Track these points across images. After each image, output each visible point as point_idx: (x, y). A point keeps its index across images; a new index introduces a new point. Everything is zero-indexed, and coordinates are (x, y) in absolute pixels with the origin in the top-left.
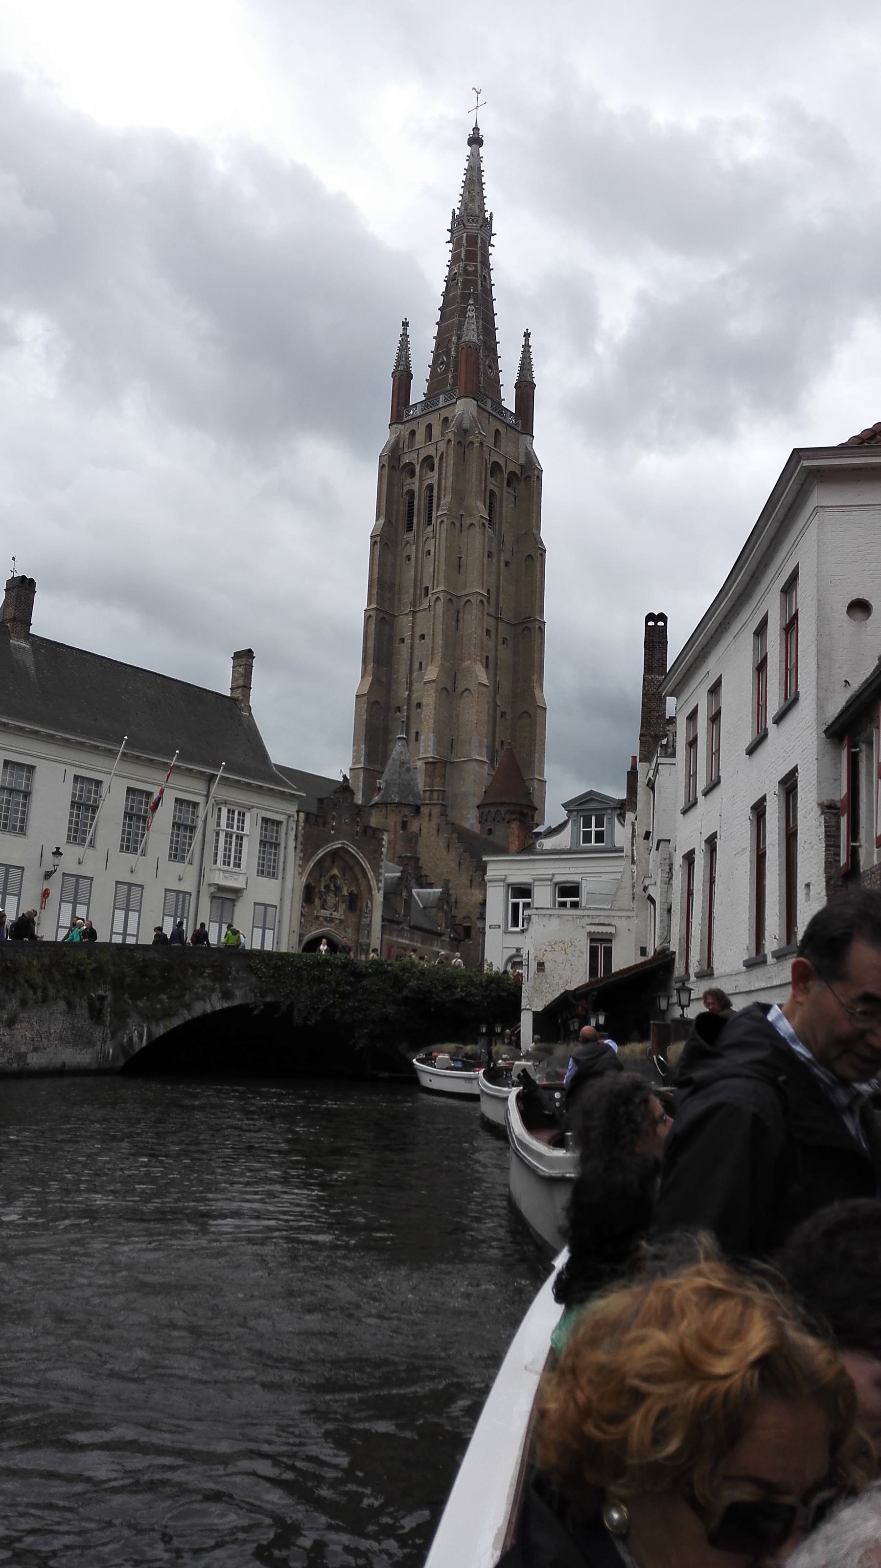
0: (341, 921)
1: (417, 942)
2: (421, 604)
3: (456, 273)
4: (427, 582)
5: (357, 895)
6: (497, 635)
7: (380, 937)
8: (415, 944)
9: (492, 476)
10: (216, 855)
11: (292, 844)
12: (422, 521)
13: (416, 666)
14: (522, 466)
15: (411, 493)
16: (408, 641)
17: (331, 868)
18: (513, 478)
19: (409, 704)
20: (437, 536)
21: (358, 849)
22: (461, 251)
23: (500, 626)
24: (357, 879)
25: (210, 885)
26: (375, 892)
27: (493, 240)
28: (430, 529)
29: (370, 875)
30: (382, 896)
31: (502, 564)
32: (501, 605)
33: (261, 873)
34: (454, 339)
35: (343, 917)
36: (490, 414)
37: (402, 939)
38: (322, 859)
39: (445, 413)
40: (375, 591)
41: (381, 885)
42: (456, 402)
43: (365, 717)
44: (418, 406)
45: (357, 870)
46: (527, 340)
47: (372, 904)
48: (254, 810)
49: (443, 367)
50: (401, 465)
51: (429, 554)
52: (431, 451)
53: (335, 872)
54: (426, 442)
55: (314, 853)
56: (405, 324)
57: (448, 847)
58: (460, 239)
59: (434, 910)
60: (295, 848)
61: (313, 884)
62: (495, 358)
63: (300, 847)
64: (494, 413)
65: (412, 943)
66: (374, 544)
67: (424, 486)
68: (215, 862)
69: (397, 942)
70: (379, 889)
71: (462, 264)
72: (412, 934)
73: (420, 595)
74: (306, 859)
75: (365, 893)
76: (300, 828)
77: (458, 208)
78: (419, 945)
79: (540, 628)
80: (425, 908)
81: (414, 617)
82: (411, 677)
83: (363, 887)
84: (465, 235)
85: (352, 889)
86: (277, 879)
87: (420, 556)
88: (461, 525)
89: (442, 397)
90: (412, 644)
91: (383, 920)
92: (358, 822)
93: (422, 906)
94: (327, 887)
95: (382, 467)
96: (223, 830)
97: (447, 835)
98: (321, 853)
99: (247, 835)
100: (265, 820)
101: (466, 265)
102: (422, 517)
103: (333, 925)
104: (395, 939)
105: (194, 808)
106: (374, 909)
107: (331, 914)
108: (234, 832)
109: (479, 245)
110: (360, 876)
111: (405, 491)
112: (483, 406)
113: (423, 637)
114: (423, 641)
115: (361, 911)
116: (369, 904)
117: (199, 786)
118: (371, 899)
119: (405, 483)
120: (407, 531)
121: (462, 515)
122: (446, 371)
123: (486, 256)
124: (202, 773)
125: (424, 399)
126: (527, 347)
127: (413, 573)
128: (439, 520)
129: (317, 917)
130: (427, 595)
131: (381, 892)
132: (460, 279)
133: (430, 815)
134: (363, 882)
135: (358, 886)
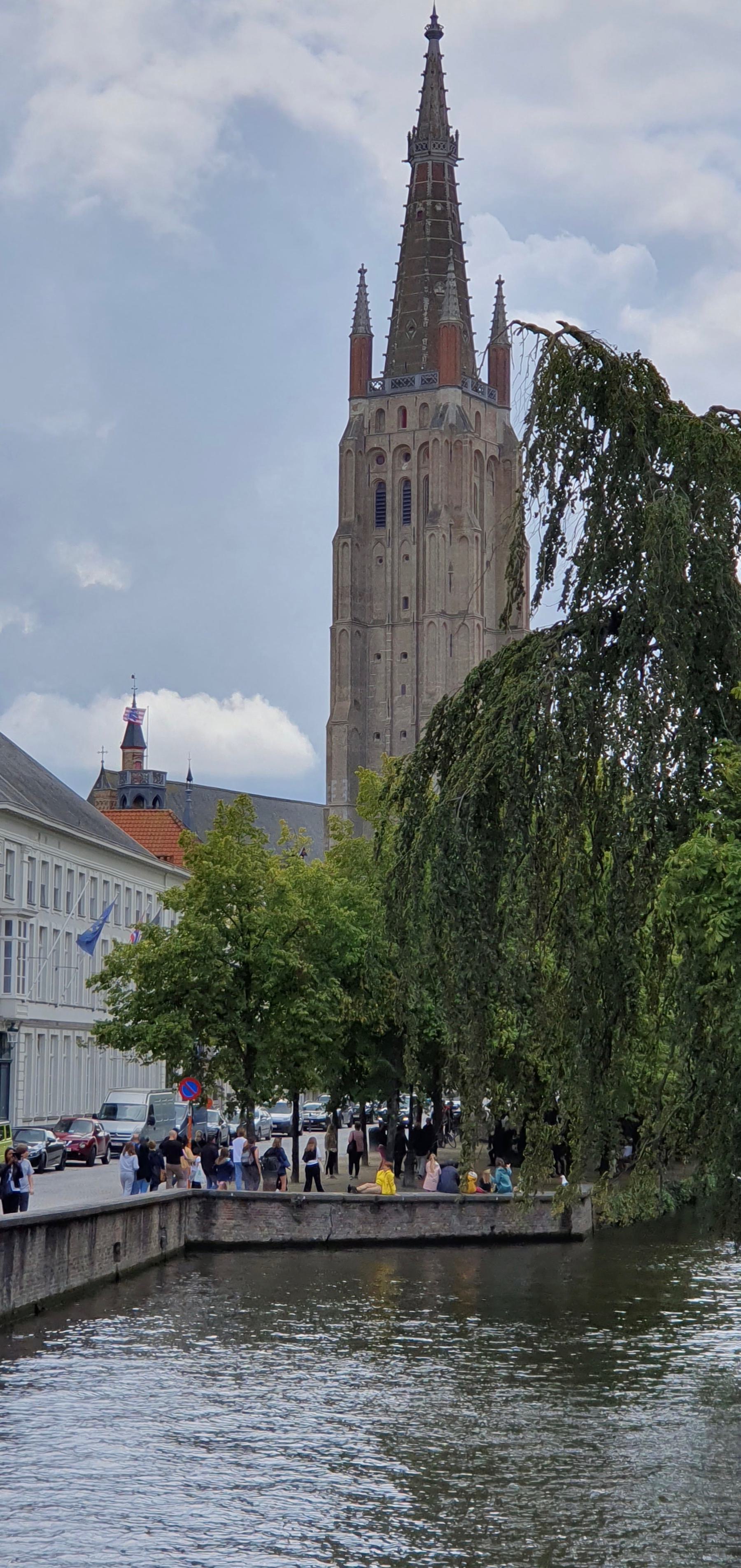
12: (397, 521)
13: (398, 688)
15: (381, 484)
34: (426, 301)
39: (423, 398)
42: (438, 389)
52: (407, 439)
67: (397, 480)
71: (429, 203)
84: (430, 163)
87: (396, 560)
89: (418, 379)
101: (434, 204)
109: (447, 177)
111: (372, 479)
113: (405, 655)
114: (404, 660)
122: (419, 337)
127: (389, 580)
132: (429, 223)
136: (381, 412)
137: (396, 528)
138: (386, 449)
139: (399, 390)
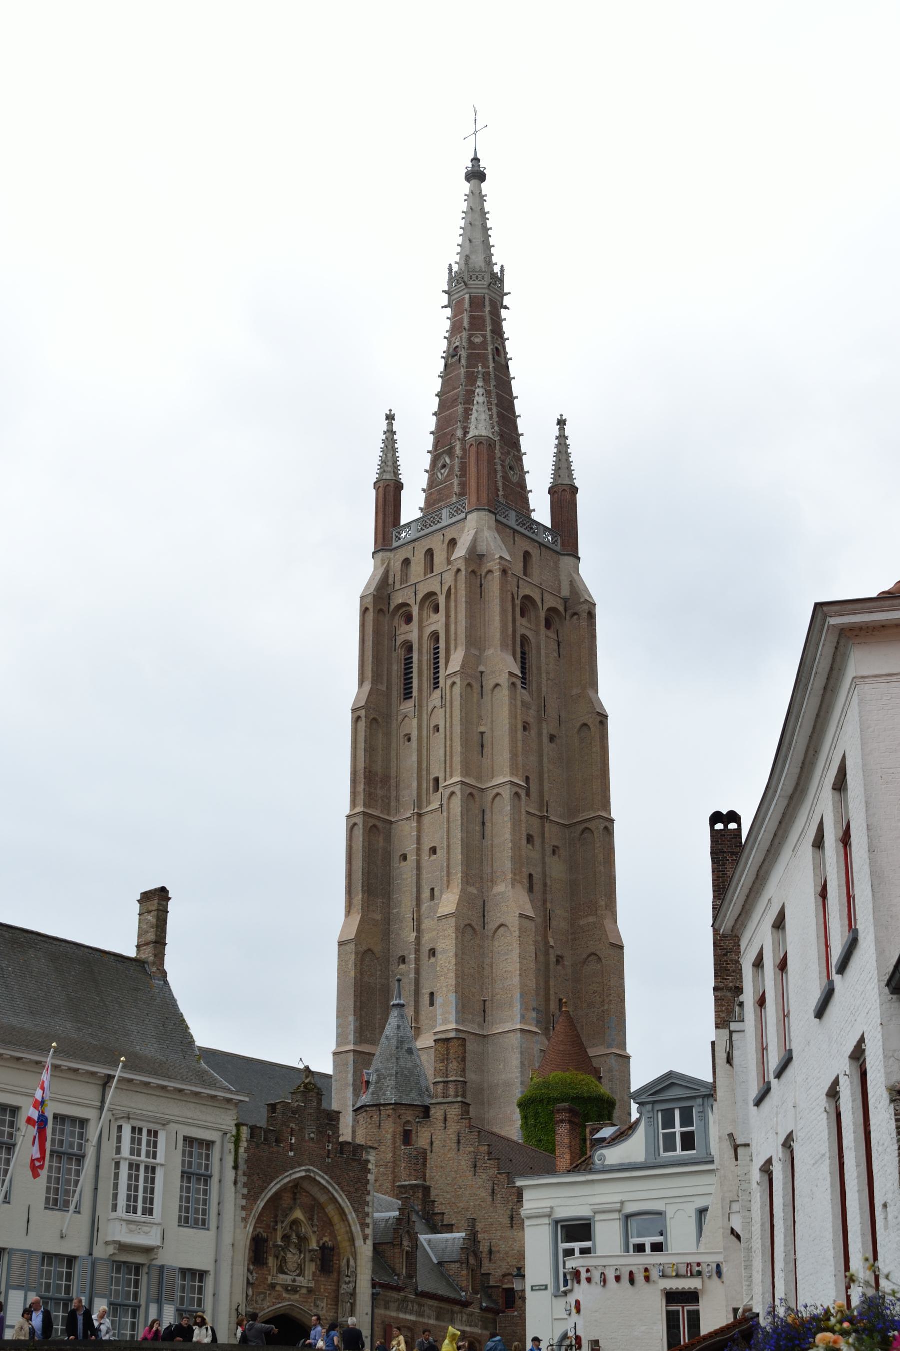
0: (310, 1291)
1: (429, 1318)
2: (429, 803)
3: (457, 347)
4: (437, 770)
5: (332, 1249)
6: (543, 842)
7: (370, 1313)
8: (426, 1321)
9: (523, 615)
10: (115, 1196)
11: (230, 1175)
14: (566, 601)
15: (408, 647)
16: (412, 858)
17: (291, 1209)
18: (552, 619)
19: (417, 951)
20: (448, 704)
21: (331, 1177)
22: (462, 318)
23: (547, 829)
24: (331, 1224)
25: (107, 1243)
26: (359, 1242)
27: (507, 301)
28: (437, 693)
29: (352, 1216)
30: (371, 1248)
31: (546, 739)
32: (546, 798)
33: (184, 1221)
34: (459, 433)
35: (312, 1285)
36: (515, 531)
37: (406, 1313)
38: (277, 1197)
40: (361, 787)
41: (369, 1231)
42: (466, 518)
43: (353, 974)
44: (413, 525)
45: (331, 1210)
46: (562, 430)
47: (355, 1260)
48: (173, 1127)
49: (446, 472)
50: (392, 607)
51: (438, 730)
53: (298, 1214)
54: (425, 575)
55: (263, 1189)
56: (390, 418)
57: (475, 1166)
58: (460, 302)
59: (454, 1266)
60: (236, 1183)
61: (265, 1235)
62: (518, 457)
63: (243, 1179)
64: (522, 530)
65: (421, 1320)
66: (356, 720)
68: (115, 1208)
69: (398, 1318)
70: (366, 1238)
71: (465, 334)
72: (421, 1305)
73: (428, 789)
74: (252, 1197)
75: (345, 1245)
76: (242, 1150)
77: (456, 263)
78: (432, 1322)
79: (606, 828)
80: (440, 1264)
81: (419, 822)
82: (419, 911)
83: (342, 1237)
84: (467, 296)
85: (325, 1239)
86: (208, 1229)
87: (425, 733)
88: (482, 686)
89: (445, 512)
90: (419, 862)
91: (374, 1285)
92: (329, 1136)
93: (436, 1262)
94: (286, 1238)
95: (364, 611)
96: (126, 1159)
97: (472, 1149)
98: (274, 1188)
99: (162, 1165)
100: (189, 1141)
101: (471, 336)
102: (425, 678)
103: (297, 1297)
104: (394, 1314)
105: (82, 1127)
106: (358, 1269)
107: (294, 1281)
108: (142, 1162)
109: (488, 309)
110: (336, 1219)
111: (398, 643)
112: (505, 521)
113: (434, 850)
114: (434, 857)
115: (339, 1273)
116: (352, 1262)
117: (91, 1093)
118: (355, 1255)
119: (397, 634)
120: (405, 699)
121: (482, 673)
123: (497, 323)
124: (93, 1074)
125: (419, 515)
126: (562, 439)
127: (415, 758)
128: (449, 682)
129: (273, 1286)
130: (437, 789)
131: (370, 1242)
133: (445, 1119)
134: (340, 1228)
135: (333, 1236)
136: (407, 562)
137: (425, 694)
138: (411, 602)
139: (427, 531)
